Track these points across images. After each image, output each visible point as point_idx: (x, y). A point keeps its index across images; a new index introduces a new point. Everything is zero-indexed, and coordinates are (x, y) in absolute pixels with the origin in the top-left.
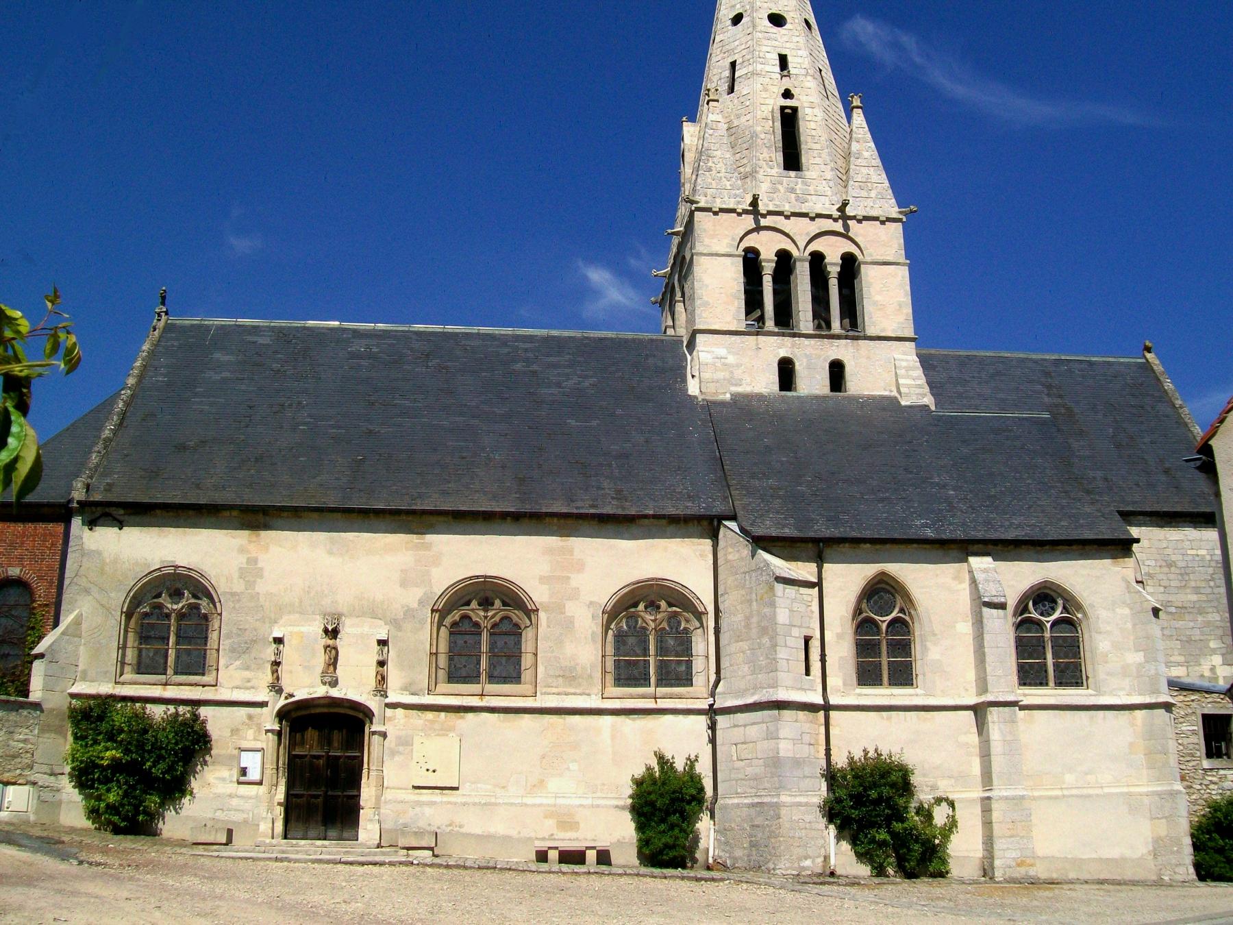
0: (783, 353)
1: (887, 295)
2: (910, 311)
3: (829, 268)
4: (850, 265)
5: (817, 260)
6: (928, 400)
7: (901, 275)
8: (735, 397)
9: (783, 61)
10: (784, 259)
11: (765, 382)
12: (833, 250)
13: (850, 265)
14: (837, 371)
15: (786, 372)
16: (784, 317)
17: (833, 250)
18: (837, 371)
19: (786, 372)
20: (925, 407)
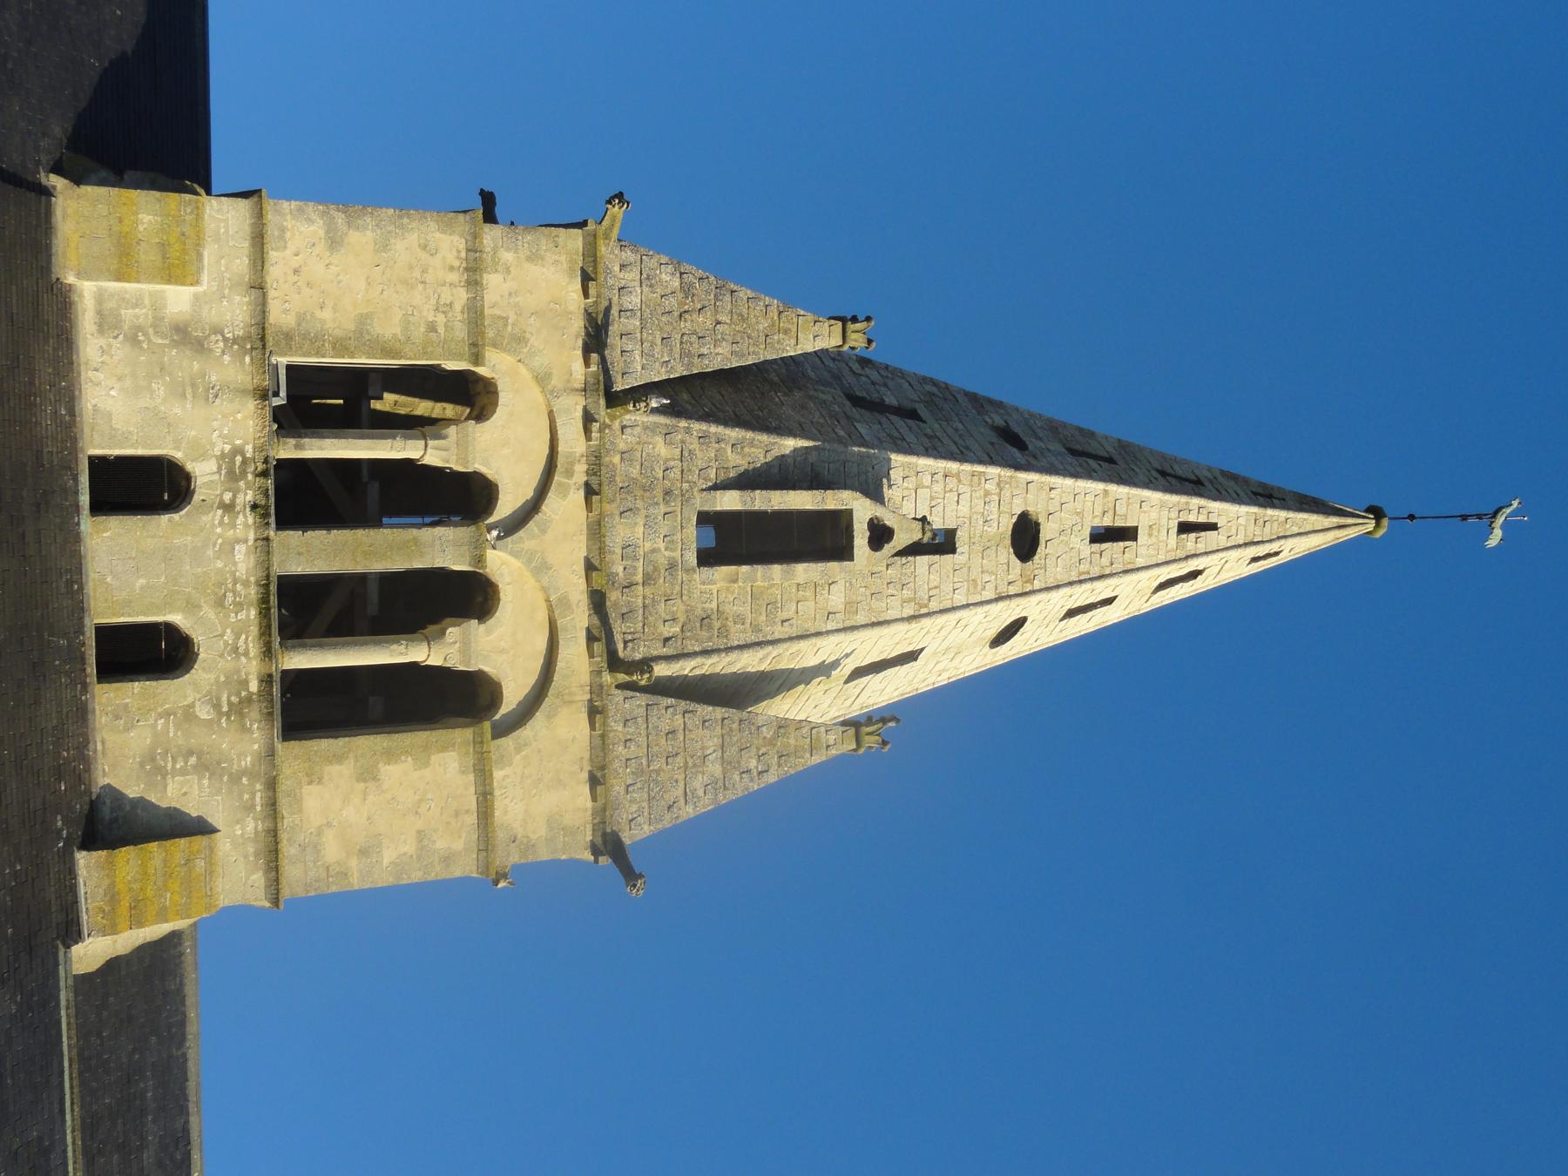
0: (204, 472)
1: (383, 810)
2: (356, 883)
3: (453, 632)
4: (458, 699)
5: (469, 596)
6: (89, 954)
7: (452, 851)
8: (63, 301)
9: (943, 543)
10: (464, 497)
11: (117, 410)
12: (497, 648)
13: (458, 699)
14: (151, 652)
15: (146, 486)
16: (301, 497)
17: (497, 648)
18: (151, 652)
19: (146, 486)
20: (71, 932)
